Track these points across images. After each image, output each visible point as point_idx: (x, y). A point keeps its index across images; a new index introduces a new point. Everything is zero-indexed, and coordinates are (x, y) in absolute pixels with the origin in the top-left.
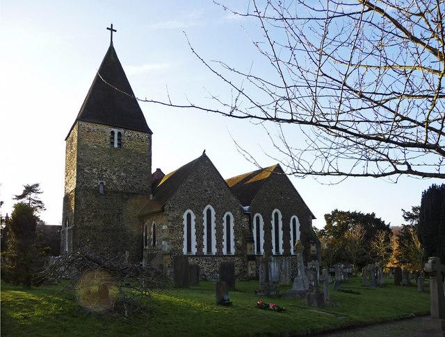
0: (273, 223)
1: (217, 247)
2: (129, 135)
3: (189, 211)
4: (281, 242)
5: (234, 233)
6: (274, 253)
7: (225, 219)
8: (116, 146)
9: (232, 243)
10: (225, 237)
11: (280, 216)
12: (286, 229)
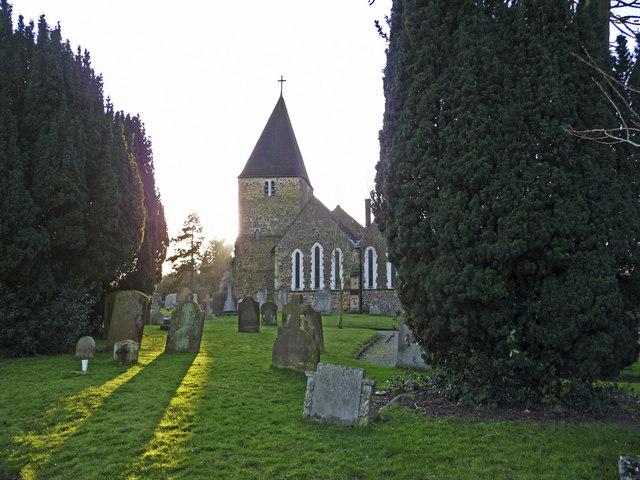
1: (325, 282)
8: (270, 195)
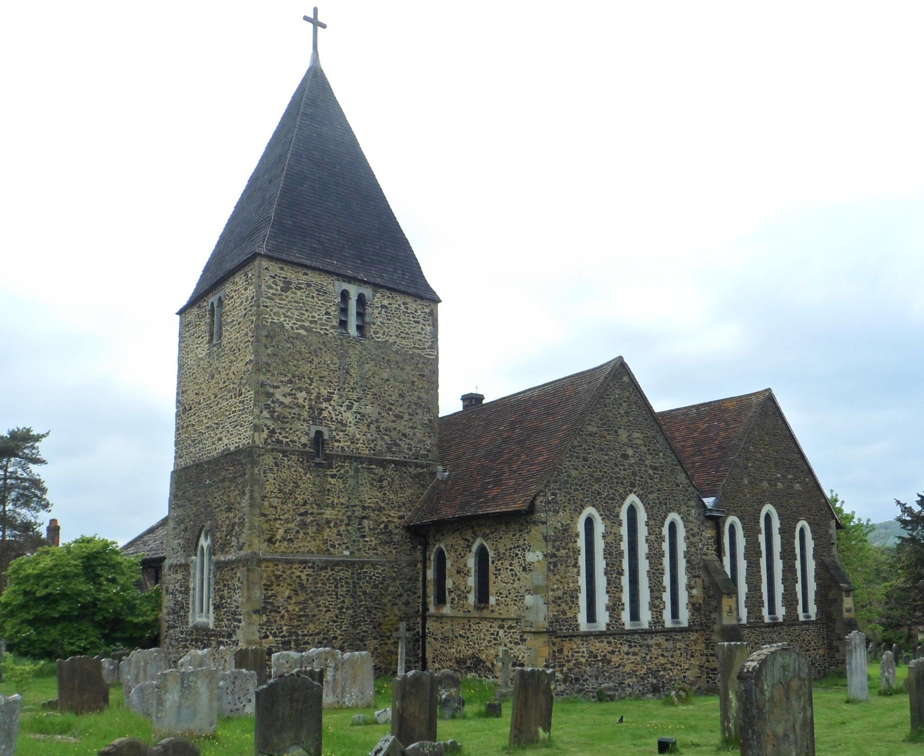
0: (762, 538)
2: (385, 302)
3: (589, 510)
4: (779, 589)
5: (687, 568)
6: (767, 619)
7: (665, 531)
9: (683, 597)
11: (776, 524)
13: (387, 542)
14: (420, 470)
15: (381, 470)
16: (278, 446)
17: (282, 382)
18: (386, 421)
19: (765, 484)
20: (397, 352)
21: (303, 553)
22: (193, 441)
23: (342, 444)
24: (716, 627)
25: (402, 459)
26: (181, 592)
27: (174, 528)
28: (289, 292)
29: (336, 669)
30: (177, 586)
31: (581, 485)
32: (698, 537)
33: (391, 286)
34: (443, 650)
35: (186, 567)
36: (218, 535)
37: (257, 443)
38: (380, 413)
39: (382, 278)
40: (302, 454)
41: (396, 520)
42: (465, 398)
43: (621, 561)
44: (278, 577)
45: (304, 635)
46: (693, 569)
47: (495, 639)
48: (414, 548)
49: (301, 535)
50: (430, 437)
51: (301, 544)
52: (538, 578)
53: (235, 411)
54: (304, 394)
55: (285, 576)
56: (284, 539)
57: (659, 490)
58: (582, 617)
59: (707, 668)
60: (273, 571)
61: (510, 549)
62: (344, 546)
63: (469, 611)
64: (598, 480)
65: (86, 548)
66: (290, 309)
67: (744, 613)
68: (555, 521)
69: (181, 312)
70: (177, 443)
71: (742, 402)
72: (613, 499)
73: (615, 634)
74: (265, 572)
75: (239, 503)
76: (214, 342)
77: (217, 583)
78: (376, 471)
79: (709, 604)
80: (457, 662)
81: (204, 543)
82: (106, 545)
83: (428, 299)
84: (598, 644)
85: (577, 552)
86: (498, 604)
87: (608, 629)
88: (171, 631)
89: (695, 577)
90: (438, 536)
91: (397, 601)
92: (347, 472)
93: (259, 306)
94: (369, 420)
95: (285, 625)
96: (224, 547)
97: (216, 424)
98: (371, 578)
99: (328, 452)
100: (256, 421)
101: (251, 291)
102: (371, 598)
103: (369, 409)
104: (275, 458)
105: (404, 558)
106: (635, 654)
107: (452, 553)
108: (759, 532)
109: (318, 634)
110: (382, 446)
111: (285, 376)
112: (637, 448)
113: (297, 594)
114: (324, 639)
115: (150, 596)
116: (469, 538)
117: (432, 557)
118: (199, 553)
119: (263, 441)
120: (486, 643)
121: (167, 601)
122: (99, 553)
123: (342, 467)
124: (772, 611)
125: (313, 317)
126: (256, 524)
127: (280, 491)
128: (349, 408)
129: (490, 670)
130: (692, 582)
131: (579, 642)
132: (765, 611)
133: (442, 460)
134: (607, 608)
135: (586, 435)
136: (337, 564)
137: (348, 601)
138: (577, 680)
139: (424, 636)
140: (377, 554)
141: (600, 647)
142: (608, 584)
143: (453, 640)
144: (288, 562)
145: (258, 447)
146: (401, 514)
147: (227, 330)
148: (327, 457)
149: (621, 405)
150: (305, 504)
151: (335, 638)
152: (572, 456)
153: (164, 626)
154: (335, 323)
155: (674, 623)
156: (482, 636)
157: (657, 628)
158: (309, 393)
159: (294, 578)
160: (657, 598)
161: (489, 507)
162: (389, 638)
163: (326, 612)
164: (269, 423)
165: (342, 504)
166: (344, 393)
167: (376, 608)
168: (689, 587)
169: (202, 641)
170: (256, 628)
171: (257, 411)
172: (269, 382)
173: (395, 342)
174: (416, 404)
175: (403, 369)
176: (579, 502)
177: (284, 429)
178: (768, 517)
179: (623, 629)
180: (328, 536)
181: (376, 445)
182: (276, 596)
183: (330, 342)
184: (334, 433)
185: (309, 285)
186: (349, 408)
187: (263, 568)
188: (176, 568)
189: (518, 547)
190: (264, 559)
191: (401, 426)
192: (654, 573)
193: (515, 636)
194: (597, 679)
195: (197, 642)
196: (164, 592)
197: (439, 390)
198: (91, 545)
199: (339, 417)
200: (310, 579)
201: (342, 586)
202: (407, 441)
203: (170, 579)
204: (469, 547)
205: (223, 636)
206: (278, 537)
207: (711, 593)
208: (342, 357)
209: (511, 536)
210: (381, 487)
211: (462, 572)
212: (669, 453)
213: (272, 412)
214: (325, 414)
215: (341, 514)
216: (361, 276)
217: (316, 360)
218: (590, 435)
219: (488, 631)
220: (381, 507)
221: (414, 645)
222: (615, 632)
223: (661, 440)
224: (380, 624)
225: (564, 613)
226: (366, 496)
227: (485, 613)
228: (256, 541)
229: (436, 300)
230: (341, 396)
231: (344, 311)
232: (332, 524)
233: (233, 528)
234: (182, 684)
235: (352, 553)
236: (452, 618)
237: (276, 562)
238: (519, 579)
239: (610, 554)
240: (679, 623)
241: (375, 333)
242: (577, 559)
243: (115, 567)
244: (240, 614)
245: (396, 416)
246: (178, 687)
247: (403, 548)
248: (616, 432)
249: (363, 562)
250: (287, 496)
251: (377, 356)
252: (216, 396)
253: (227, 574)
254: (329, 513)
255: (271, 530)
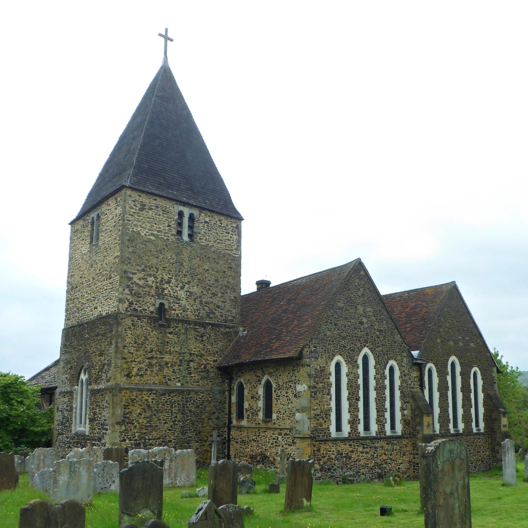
2: (207, 219)
3: (338, 358)
5: (401, 397)
7: (387, 372)
10: (387, 405)
11: (458, 369)
12: (466, 389)
13: (206, 378)
14: (228, 330)
15: (203, 329)
16: (134, 313)
17: (138, 270)
18: (206, 297)
19: (451, 343)
20: (214, 252)
21: (150, 384)
22: (78, 309)
23: (177, 312)
24: (420, 436)
25: (217, 322)
26: (67, 410)
27: (63, 367)
28: (144, 212)
29: (171, 461)
30: (65, 406)
31: (333, 341)
32: (408, 377)
33: (210, 208)
34: (242, 450)
35: (71, 393)
36: (93, 372)
37: (121, 310)
38: (202, 292)
39: (206, 203)
40: (150, 318)
41: (212, 363)
42: (258, 283)
43: (358, 391)
44: (133, 400)
45: (150, 439)
46: (405, 397)
47: (276, 442)
48: (223, 382)
49: (148, 372)
50: (235, 308)
51: (148, 378)
52: (304, 402)
53: (106, 289)
54: (152, 279)
55: (137, 399)
56: (137, 375)
57: (383, 345)
58: (333, 428)
59: (414, 463)
60: (130, 396)
61: (286, 382)
62: (177, 380)
63: (259, 424)
64: (344, 338)
65: (4, 380)
66: (144, 222)
67: (437, 426)
68: (316, 365)
69: (72, 223)
70: (67, 310)
71: (437, 290)
72: (354, 351)
73: (354, 440)
74: (125, 396)
75: (108, 350)
76: (94, 243)
77: (92, 404)
78: (199, 330)
79: (415, 420)
80: (251, 458)
81: (84, 377)
82: (17, 378)
83: (235, 218)
84: (343, 446)
85: (330, 385)
86: (278, 419)
87: (350, 436)
88: (60, 437)
89: (405, 402)
90: (239, 374)
91: (212, 417)
92: (180, 330)
93: (124, 220)
94: (195, 296)
95: (137, 432)
96: (97, 380)
97: (94, 297)
98: (194, 401)
99: (167, 317)
100: (121, 296)
101: (119, 211)
102: (194, 414)
103: (195, 289)
104: (132, 321)
105: (217, 388)
106: (367, 453)
107: (248, 385)
108: (448, 374)
109: (159, 438)
110: (203, 313)
111: (140, 266)
112: (369, 318)
113: (145, 412)
114: (163, 442)
115: (46, 413)
116: (259, 375)
117: (235, 388)
118: (80, 384)
119: (125, 309)
120: (269, 445)
121: (58, 416)
122: (12, 384)
123: (177, 327)
124: (455, 425)
125: (160, 228)
126: (119, 365)
127: (136, 342)
128: (182, 288)
129: (272, 463)
130: (404, 406)
131: (331, 445)
132: (451, 426)
133: (242, 324)
134: (349, 422)
135: (336, 308)
136: (172, 391)
137: (179, 416)
138: (329, 469)
139: (229, 441)
140: (199, 385)
141: (345, 448)
142: (350, 406)
143: (248, 443)
144: (139, 390)
145: (121, 313)
146: (215, 359)
147: (102, 236)
148: (168, 321)
149: (359, 289)
150: (152, 351)
151: (170, 441)
152: (327, 322)
153: (56, 433)
154: (174, 232)
155: (392, 432)
156: (268, 440)
157: (381, 436)
158: (156, 278)
159: (144, 401)
160: (381, 416)
161: (272, 354)
162: (206, 441)
163: (164, 424)
164: (129, 297)
165: (176, 352)
166: (179, 278)
167: (198, 421)
168: (402, 409)
169: (81, 444)
170: (118, 434)
171: (121, 289)
172: (130, 270)
173: (213, 246)
174: (226, 286)
175: (218, 263)
176: (331, 352)
177: (138, 301)
178: (453, 365)
179: (360, 437)
180: (166, 373)
181: (199, 313)
182: (131, 413)
183: (170, 245)
184: (172, 305)
185: (157, 207)
186: (182, 288)
187: (123, 394)
188: (64, 394)
189: (292, 381)
190: (124, 388)
191: (216, 300)
192: (379, 400)
193: (288, 440)
194: (342, 469)
195: (77, 444)
196: (56, 410)
197: (242, 278)
198: (7, 378)
199: (176, 294)
200: (154, 401)
201: (175, 406)
202: (220, 310)
203: (60, 401)
204: (260, 381)
205: (95, 440)
206: (134, 373)
207: (416, 413)
208: (178, 254)
209: (287, 374)
210: (203, 341)
211: (254, 398)
212: (389, 321)
213: (131, 290)
214: (166, 292)
215: (175, 358)
216: (192, 202)
217: (161, 257)
218: (339, 309)
219: (271, 437)
220: (202, 354)
221: (222, 447)
222: (354, 438)
223: (385, 313)
224: (200, 432)
225: (321, 425)
226: (193, 347)
227: (270, 425)
228: (119, 376)
229: (241, 219)
230: (177, 280)
231: (180, 224)
232: (169, 365)
233: (103, 367)
234: (70, 469)
235: (182, 384)
236: (248, 428)
237: (132, 390)
238: (292, 403)
239: (351, 386)
240: (395, 432)
241: (200, 239)
242: (329, 390)
243: (22, 393)
244: (107, 425)
245: (213, 294)
246: (67, 471)
247: (216, 381)
248: (356, 307)
249: (190, 391)
250: (139, 346)
251: (201, 254)
252: (94, 279)
253: (99, 398)
254: (167, 358)
255: (129, 368)
